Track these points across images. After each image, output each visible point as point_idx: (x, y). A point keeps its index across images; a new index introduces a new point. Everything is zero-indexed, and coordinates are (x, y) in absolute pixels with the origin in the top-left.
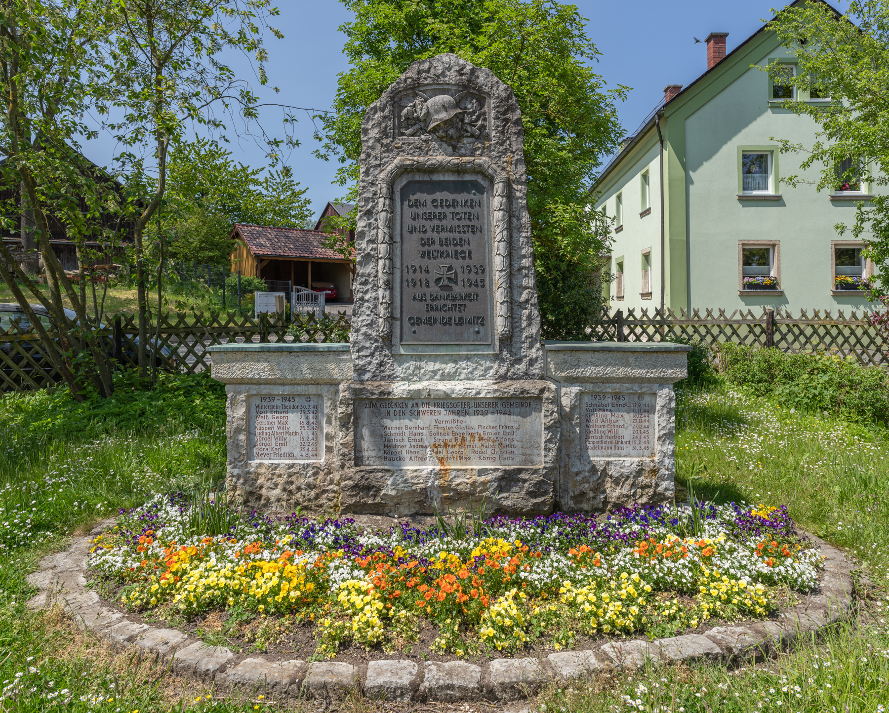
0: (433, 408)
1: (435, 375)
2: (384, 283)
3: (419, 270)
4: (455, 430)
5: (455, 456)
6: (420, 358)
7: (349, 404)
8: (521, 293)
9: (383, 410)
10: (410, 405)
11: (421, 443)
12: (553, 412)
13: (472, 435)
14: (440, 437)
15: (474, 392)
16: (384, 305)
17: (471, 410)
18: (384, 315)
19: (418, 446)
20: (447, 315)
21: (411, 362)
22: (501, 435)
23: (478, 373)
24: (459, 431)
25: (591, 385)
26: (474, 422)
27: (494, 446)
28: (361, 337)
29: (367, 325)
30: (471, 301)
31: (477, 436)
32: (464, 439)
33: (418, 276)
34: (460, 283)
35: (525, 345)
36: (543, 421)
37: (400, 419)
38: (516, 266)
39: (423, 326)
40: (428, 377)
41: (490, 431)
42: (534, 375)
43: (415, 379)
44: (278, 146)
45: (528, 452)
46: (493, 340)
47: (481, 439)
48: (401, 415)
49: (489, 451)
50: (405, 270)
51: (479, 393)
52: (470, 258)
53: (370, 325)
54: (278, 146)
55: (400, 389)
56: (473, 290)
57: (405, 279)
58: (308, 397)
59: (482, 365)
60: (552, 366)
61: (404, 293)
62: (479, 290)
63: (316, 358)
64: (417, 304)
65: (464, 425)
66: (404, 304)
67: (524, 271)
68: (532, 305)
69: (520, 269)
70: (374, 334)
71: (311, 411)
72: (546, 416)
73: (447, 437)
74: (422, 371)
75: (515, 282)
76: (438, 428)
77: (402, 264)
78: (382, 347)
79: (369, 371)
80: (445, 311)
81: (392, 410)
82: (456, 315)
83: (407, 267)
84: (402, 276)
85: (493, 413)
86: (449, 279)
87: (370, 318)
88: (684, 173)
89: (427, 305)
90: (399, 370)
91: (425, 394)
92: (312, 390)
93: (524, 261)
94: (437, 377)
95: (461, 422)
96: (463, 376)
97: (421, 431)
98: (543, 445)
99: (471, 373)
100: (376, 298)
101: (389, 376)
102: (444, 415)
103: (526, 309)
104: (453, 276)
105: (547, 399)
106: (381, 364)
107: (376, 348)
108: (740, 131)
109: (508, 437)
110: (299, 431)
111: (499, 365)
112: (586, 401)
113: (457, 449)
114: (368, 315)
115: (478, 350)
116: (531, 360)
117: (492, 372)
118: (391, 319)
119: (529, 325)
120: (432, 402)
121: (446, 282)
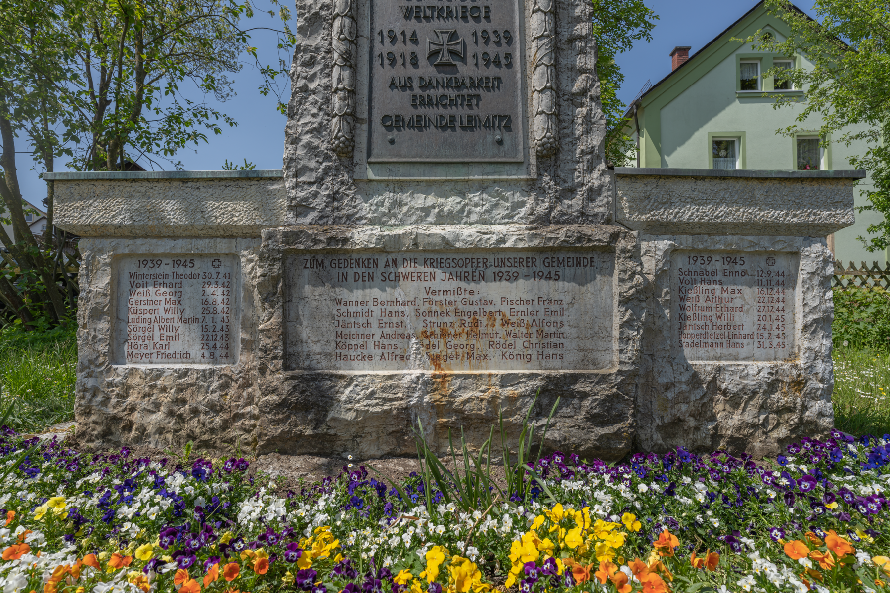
0: (422, 269)
1: (427, 216)
2: (341, 55)
3: (400, 38)
4: (461, 307)
5: (460, 351)
6: (401, 186)
7: (275, 260)
8: (573, 80)
9: (335, 272)
10: (382, 264)
11: (400, 330)
12: (634, 273)
13: (491, 316)
14: (434, 320)
15: (495, 238)
16: (341, 94)
17: (489, 272)
18: (340, 109)
19: (395, 335)
20: (447, 112)
21: (387, 194)
22: (541, 315)
23: (501, 212)
24: (468, 308)
25: (690, 238)
26: (496, 292)
27: (529, 335)
28: (301, 152)
29: (311, 132)
30: (488, 89)
31: (499, 318)
32: (475, 323)
33: (398, 48)
34: (470, 60)
35: (581, 166)
36: (616, 290)
37: (364, 288)
38: (565, 35)
39: (407, 133)
40: (414, 218)
41: (522, 308)
42: (595, 216)
43: (393, 221)
45: (589, 345)
46: (526, 155)
47: (505, 322)
48: (367, 280)
49: (519, 343)
50: (378, 39)
51: (502, 240)
52: (487, 18)
53: (317, 131)
55: (363, 236)
56: (493, 71)
57: (376, 53)
58: (216, 259)
59: (506, 200)
60: (625, 204)
61: (376, 77)
62: (502, 72)
63: (227, 191)
64: (397, 94)
65: (476, 297)
66: (375, 95)
67: (579, 44)
68: (592, 98)
69: (572, 40)
70: (324, 146)
71: (220, 282)
72: (621, 280)
73: (446, 319)
74: (405, 209)
75: (563, 62)
76: (430, 302)
77: (372, 29)
78: (337, 169)
79: (314, 209)
80: (445, 106)
81: (351, 272)
82: (461, 112)
83: (381, 33)
84: (372, 49)
85: (527, 277)
86: (452, 53)
87: (318, 119)
88: (659, 157)
89: (414, 96)
90: (365, 208)
91: (408, 242)
92: (222, 246)
93: (578, 26)
94: (430, 219)
95: (471, 292)
96: (474, 218)
97: (401, 308)
98: (616, 333)
99: (488, 211)
100: (327, 87)
101: (349, 217)
102: (442, 280)
103: (582, 105)
104: (459, 48)
105: (624, 250)
106: (334, 197)
107: (327, 170)
108: (710, 119)
109: (553, 319)
110: (200, 316)
111: (536, 199)
112: (680, 265)
113: (463, 340)
114: (314, 115)
115: (500, 173)
116: (591, 190)
117: (523, 211)
118: (351, 117)
119: (588, 132)
120: (421, 259)
121: (447, 58)
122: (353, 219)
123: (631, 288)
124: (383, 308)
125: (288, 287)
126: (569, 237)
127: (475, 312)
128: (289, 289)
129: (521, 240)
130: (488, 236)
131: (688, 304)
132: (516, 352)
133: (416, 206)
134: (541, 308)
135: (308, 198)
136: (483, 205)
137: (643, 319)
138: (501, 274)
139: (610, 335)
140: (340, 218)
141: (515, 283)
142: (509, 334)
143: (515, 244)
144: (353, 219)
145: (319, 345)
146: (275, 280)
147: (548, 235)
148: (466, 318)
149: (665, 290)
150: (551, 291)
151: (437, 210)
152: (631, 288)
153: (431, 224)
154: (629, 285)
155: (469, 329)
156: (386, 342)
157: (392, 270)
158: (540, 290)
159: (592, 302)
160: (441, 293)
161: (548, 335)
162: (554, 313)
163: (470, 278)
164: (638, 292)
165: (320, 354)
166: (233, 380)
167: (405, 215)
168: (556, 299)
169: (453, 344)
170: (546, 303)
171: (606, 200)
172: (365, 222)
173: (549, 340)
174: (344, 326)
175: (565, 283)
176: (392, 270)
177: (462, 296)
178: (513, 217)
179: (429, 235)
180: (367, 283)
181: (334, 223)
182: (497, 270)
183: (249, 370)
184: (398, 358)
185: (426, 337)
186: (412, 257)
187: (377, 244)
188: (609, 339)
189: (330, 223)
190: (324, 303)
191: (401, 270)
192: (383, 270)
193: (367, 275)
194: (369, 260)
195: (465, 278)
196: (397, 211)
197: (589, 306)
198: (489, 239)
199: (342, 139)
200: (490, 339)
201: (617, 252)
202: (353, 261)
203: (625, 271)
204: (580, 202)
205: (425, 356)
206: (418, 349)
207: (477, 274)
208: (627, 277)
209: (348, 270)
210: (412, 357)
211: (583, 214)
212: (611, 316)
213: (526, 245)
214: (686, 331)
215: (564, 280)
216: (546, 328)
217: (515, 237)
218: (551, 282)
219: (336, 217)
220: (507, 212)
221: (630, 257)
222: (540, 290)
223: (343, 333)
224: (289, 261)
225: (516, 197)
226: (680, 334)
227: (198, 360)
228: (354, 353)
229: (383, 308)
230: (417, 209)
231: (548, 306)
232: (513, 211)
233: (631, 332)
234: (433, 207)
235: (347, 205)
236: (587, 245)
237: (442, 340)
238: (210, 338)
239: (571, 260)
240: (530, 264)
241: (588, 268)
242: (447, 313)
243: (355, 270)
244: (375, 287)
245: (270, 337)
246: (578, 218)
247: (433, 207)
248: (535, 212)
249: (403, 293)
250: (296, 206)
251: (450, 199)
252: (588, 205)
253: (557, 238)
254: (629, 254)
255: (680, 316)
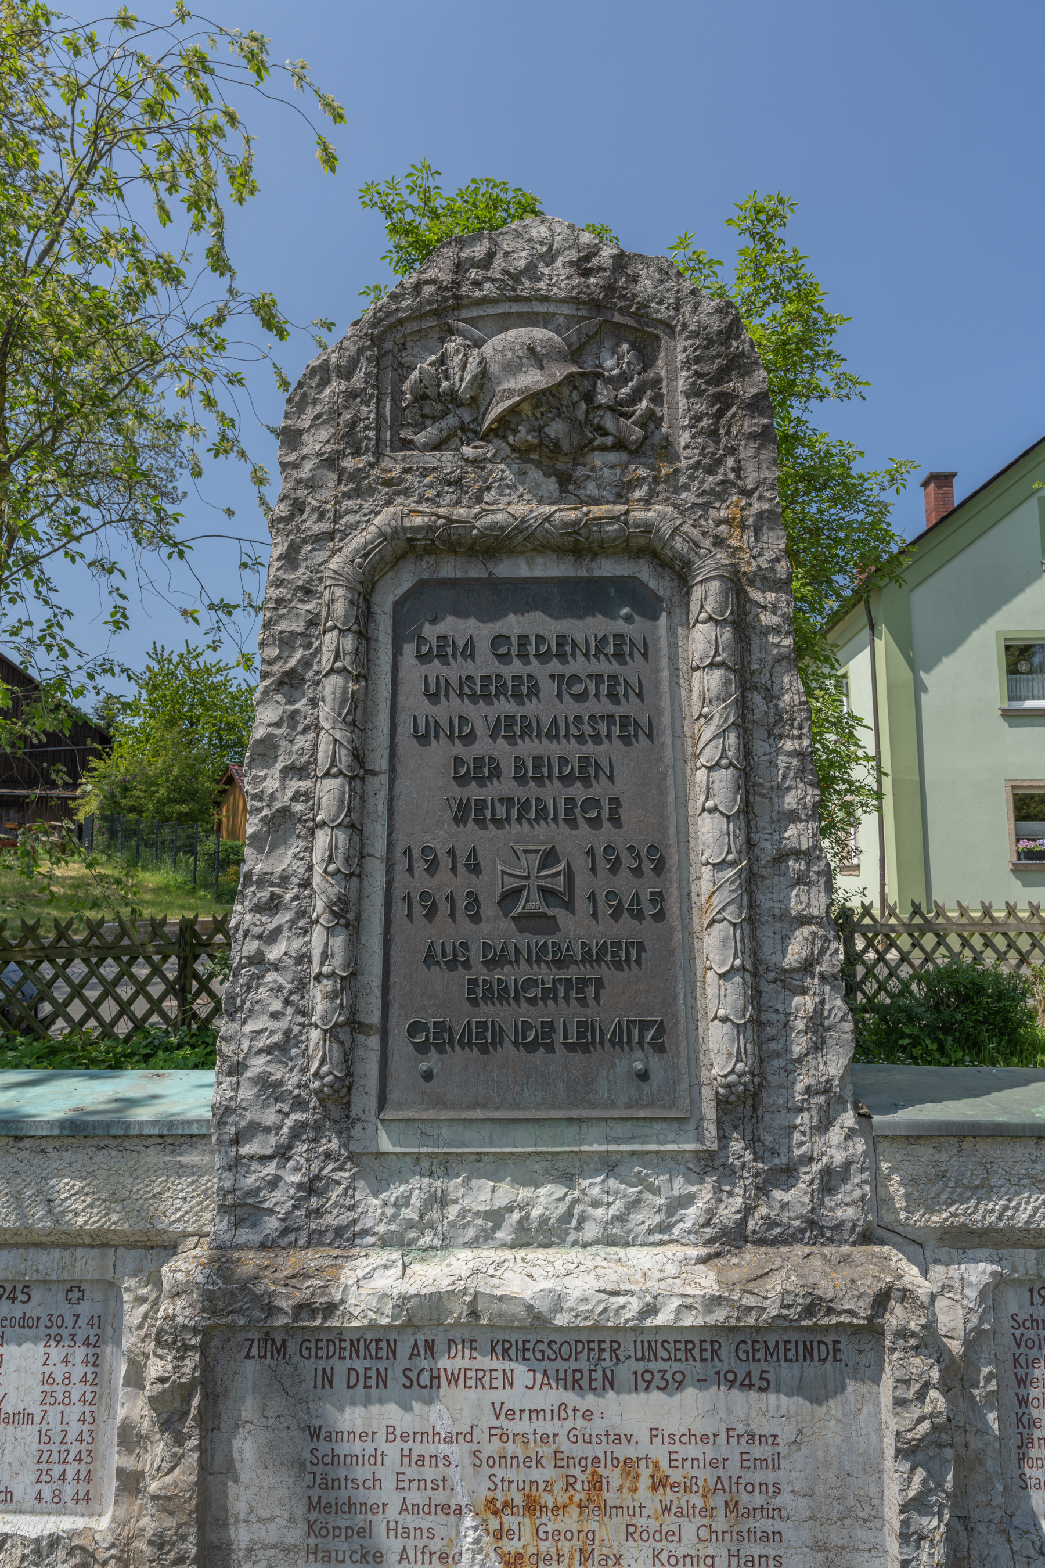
0: (485, 1362)
1: (497, 1227)
2: (329, 907)
3: (446, 862)
4: (566, 1447)
5: (565, 1546)
6: (444, 1165)
7: (186, 1348)
8: (785, 939)
9: (308, 1367)
10: (404, 1350)
11: (440, 1497)
12: (926, 1386)
13: (629, 1467)
14: (511, 1474)
15: (635, 1305)
16: (328, 984)
17: (624, 1372)
18: (325, 1018)
19: (430, 1508)
20: (538, 1016)
21: (416, 1181)
22: (733, 1468)
23: (645, 1218)
24: (581, 1450)
25: (1031, 1254)
26: (637, 1414)
27: (708, 1511)
28: (247, 1093)
29: (268, 1050)
30: (618, 966)
31: (645, 1472)
32: (596, 1484)
33: (444, 882)
34: (582, 905)
35: (804, 1120)
36: (892, 1424)
37: (367, 1402)
38: (767, 849)
39: (458, 1056)
40: (471, 1233)
41: (693, 1451)
42: (839, 1227)
43: (426, 1240)
44: (230, 613)
45: (835, 1536)
46: (695, 1103)
47: (659, 1483)
48: (373, 1385)
49: (689, 1529)
50: (401, 864)
51: (651, 1310)
52: (616, 821)
53: (280, 1050)
54: (230, 613)
56: (626, 929)
57: (398, 893)
58: (75, 1290)
59: (656, 1191)
60: (896, 1189)
61: (396, 940)
62: (646, 930)
63: (101, 1157)
64: (439, 976)
65: (597, 1427)
66: (394, 978)
67: (795, 866)
68: (823, 978)
69: (782, 857)
70: (294, 1079)
71: (80, 1337)
72: (900, 1402)
73: (535, 1474)
74: (453, 1211)
75: (765, 901)
76: (503, 1436)
77: (390, 845)
78: (318, 1127)
79: (271, 1212)
80: (532, 1001)
81: (341, 1368)
82: (568, 1015)
83: (408, 852)
84: (389, 884)
85: (702, 1383)
86: (546, 892)
87: (282, 1025)
89: (473, 982)
90: (373, 1209)
91: (458, 1310)
92: (86, 1265)
93: (791, 831)
94: (503, 1235)
95: (588, 1415)
96: (591, 1231)
97: (443, 1449)
98: (893, 1517)
99: (621, 1219)
100: (303, 958)
101: (339, 1231)
102: (525, 1389)
103: (804, 991)
104: (560, 884)
105: (903, 1333)
106: (312, 1187)
107: (296, 1132)
109: (758, 1476)
110: (36, 1410)
111: (718, 1190)
112: (1013, 1307)
113: (570, 1521)
114: (275, 1016)
115: (644, 1139)
116: (827, 1172)
117: (692, 1214)
118: (348, 1029)
119: (817, 1047)
120: (484, 1343)
121: (537, 904)
122: (349, 1234)
123: (921, 1420)
124: (406, 1447)
125: (213, 1398)
126: (788, 1307)
127: (596, 1460)
128: (215, 1403)
129: (689, 1307)
130: (621, 1300)
131: (1034, 1393)
132: (682, 1551)
133: (476, 1208)
134: (733, 1452)
135: (259, 1189)
136: (609, 1204)
137: (949, 1485)
138: (648, 1377)
139: (879, 1516)
140: (322, 1233)
141: (677, 1397)
142: (666, 1509)
143: (677, 1318)
144: (349, 1234)
145: (272, 1526)
146: (186, 1392)
147: (744, 1302)
148: (576, 1472)
149: (985, 1370)
150: (753, 1414)
151: (516, 1216)
152: (921, 1420)
153: (504, 1245)
154: (916, 1412)
155: (583, 1496)
156: (411, 1521)
157: (425, 1364)
158: (729, 1411)
159: (838, 1439)
160: (526, 1415)
161: (751, 1513)
162: (759, 1463)
163: (585, 1383)
164: (935, 1428)
165: (274, 1546)
166: (96, 1560)
167: (453, 1224)
168: (764, 1432)
169: (549, 1528)
170: (743, 1441)
171: (857, 1193)
172: (371, 1240)
173: (751, 1523)
174: (325, 1486)
175: (782, 1397)
176: (425, 1364)
177: (569, 1424)
178: (671, 1226)
179: (501, 1298)
180: (373, 1391)
181: (309, 1244)
182: (641, 1366)
183: (130, 1539)
184: (435, 1558)
185: (496, 1513)
186: (466, 1337)
187: (394, 1317)
188: (877, 1523)
189: (301, 1243)
190: (284, 1434)
191: (443, 1363)
192: (406, 1364)
193: (373, 1373)
194: (378, 1341)
195: (574, 1382)
196: (435, 1215)
197: (833, 1450)
198: (623, 1307)
199: (328, 1079)
200: (627, 1519)
201: (889, 1336)
202: (346, 1345)
203: (907, 1382)
204: (806, 1199)
205: (493, 1555)
206: (477, 1541)
207: (598, 1375)
208: (911, 1394)
209: (335, 1362)
210: (466, 1557)
211: (812, 1224)
212: (880, 1472)
213: (700, 1322)
214: (1033, 1453)
215: (778, 1391)
216: (744, 1498)
217: (676, 1302)
218: (753, 1395)
219: (314, 1231)
220: (658, 1219)
221: (917, 1348)
222: (729, 1411)
223: (323, 1502)
224: (216, 1342)
225: (676, 1186)
226: (1022, 1458)
227: (27, 1507)
228: (345, 1546)
229: (406, 1447)
230: (477, 1214)
231: (745, 1448)
232: (670, 1214)
233: (925, 1520)
234: (510, 1209)
235: (335, 1204)
236: (826, 1321)
237: (527, 1521)
238: (55, 1457)
239: (792, 1346)
240: (707, 1355)
241: (828, 1364)
242: (538, 1461)
243: (348, 1363)
244: (389, 1401)
245: (172, 1514)
246: (803, 1231)
247: (510, 1209)
248: (716, 1220)
249: (446, 1416)
250: (234, 1206)
251: (543, 1191)
252: (822, 1204)
253: (764, 1309)
254: (912, 1342)
255: (1019, 1420)
